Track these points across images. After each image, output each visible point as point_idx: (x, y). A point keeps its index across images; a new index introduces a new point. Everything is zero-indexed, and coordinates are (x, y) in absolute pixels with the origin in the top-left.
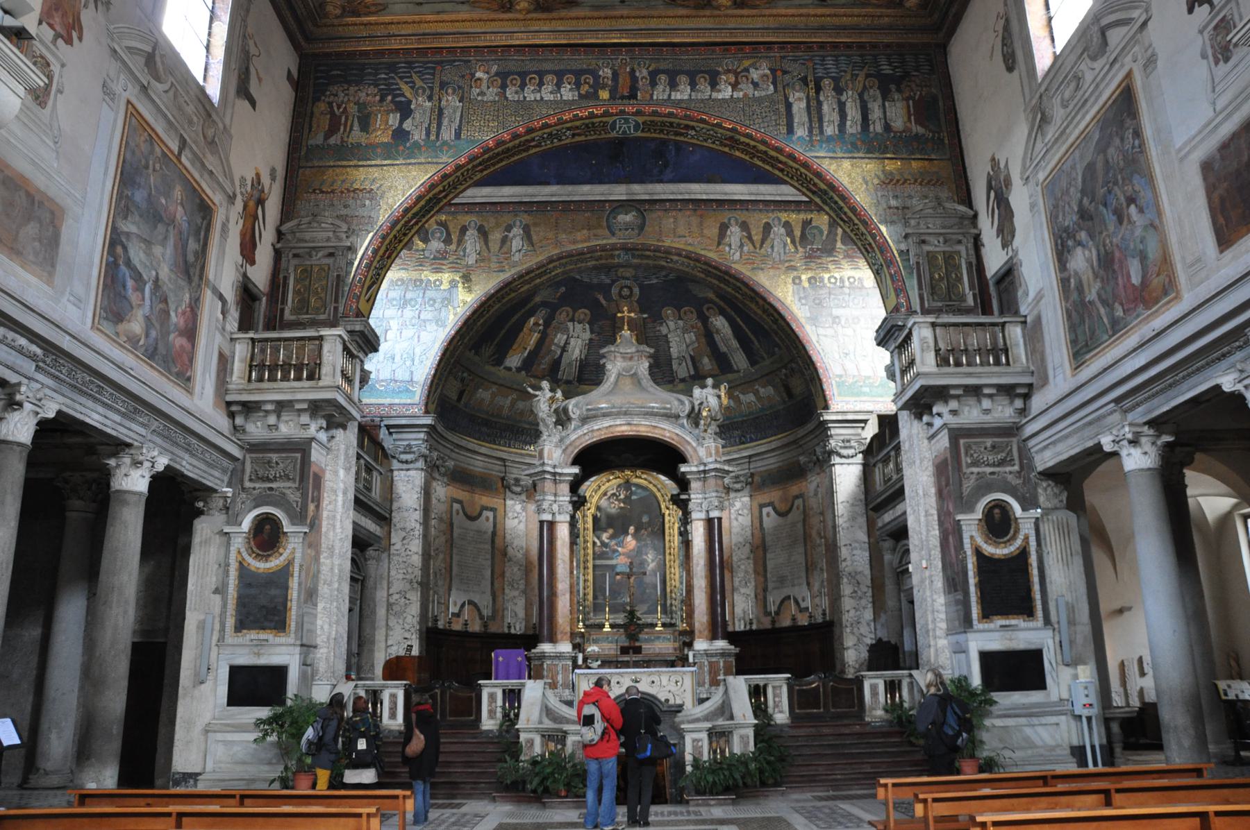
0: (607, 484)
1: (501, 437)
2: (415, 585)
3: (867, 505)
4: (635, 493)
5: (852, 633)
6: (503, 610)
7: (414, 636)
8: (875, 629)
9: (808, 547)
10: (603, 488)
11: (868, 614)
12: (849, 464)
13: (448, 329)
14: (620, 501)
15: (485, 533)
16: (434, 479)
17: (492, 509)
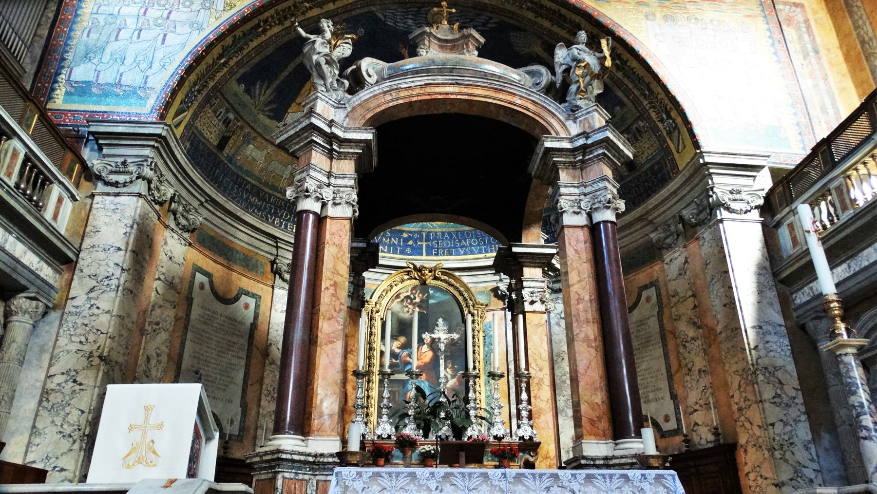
0: (400, 286)
1: (276, 214)
2: (96, 361)
3: (775, 275)
4: (432, 298)
5: (786, 461)
6: (256, 429)
7: (76, 446)
8: (818, 456)
9: (671, 346)
10: (395, 289)
11: (803, 432)
12: (743, 221)
13: (204, 34)
14: (414, 304)
15: (241, 323)
16: (167, 227)
17: (253, 296)
